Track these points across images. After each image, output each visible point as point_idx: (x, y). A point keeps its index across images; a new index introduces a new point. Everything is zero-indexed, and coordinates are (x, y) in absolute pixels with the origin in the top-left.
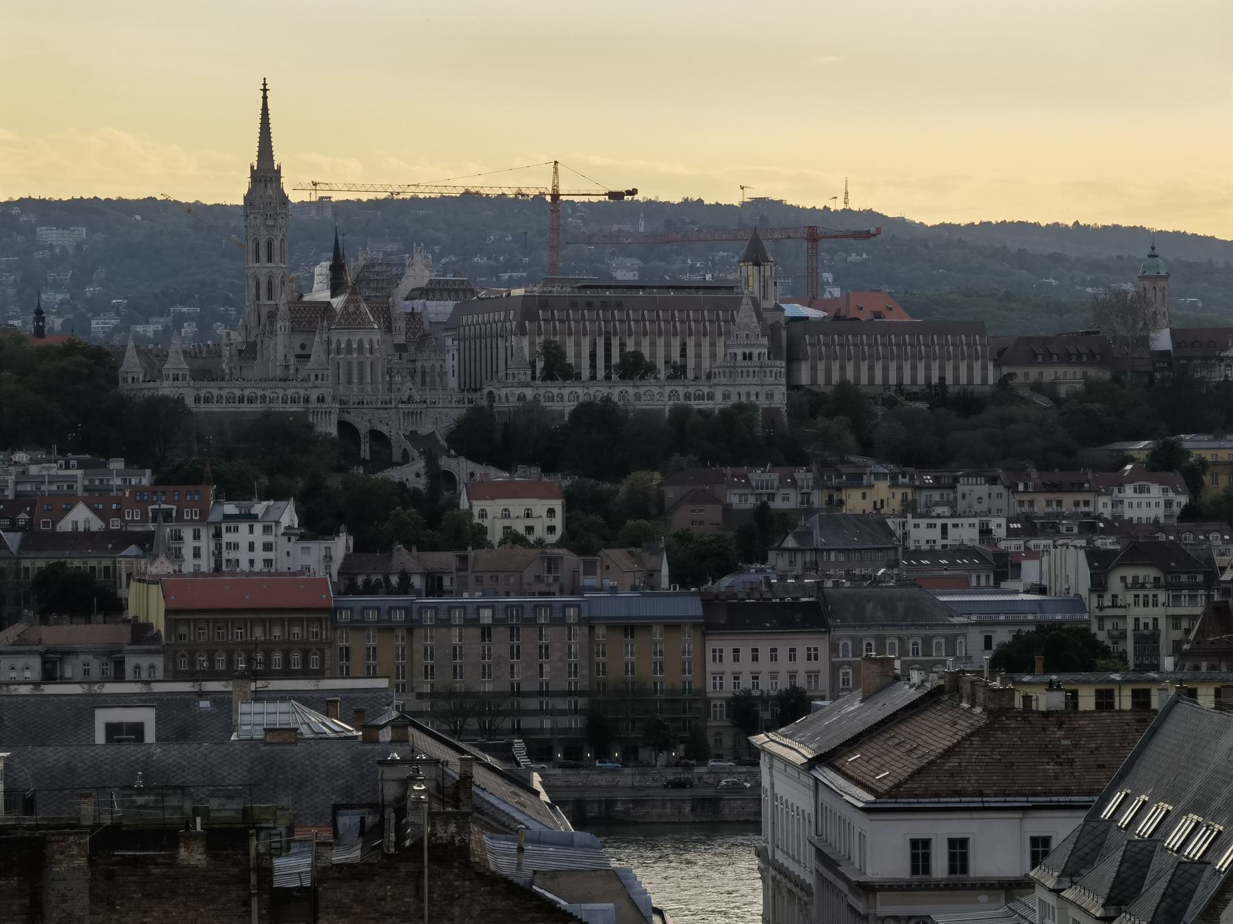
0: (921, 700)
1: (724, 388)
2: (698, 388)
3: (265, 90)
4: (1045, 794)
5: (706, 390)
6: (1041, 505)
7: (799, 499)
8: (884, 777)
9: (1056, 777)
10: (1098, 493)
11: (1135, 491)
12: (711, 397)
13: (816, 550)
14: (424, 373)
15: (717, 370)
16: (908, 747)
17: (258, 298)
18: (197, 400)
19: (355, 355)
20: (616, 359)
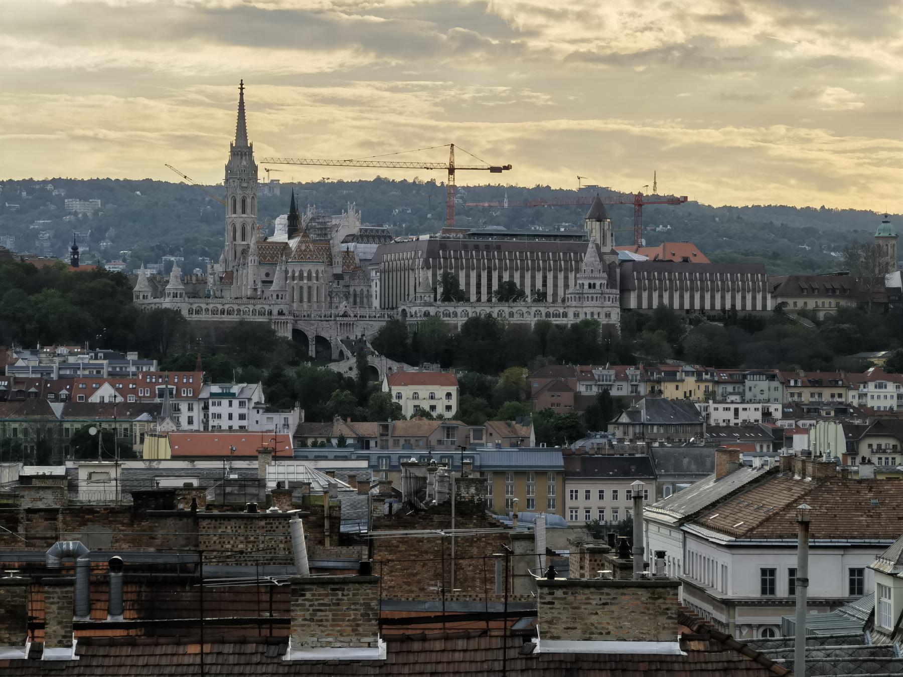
0: (762, 477)
1: (574, 309)
2: (554, 309)
3: (242, 89)
4: (861, 538)
5: (561, 311)
6: (806, 397)
7: (630, 389)
8: (740, 526)
9: (868, 526)
10: (848, 388)
11: (876, 387)
12: (565, 315)
13: (643, 424)
14: (355, 296)
15: (569, 296)
16: (756, 506)
17: (235, 239)
18: (190, 312)
19: (305, 281)
20: (495, 287)
